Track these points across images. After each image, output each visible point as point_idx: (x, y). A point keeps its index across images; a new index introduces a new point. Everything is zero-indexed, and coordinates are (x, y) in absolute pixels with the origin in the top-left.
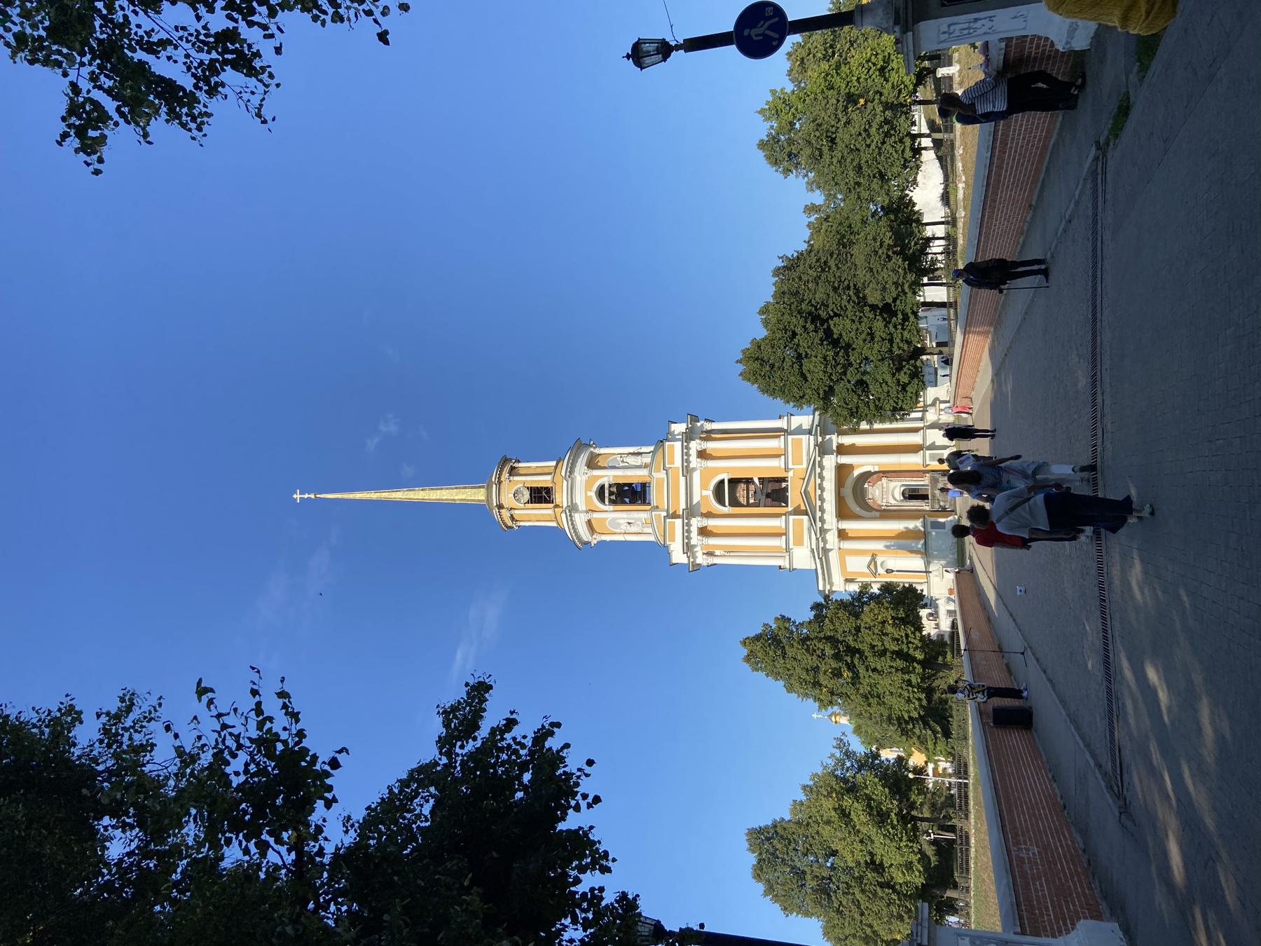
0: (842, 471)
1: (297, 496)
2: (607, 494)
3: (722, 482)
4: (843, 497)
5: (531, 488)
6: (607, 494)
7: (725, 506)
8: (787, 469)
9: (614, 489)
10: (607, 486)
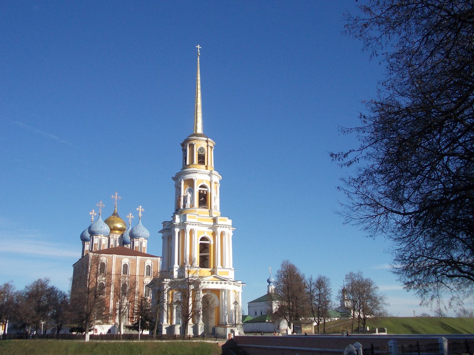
0: (217, 292)
1: (199, 47)
3: (210, 242)
5: (205, 155)
7: (201, 240)
10: (206, 189)
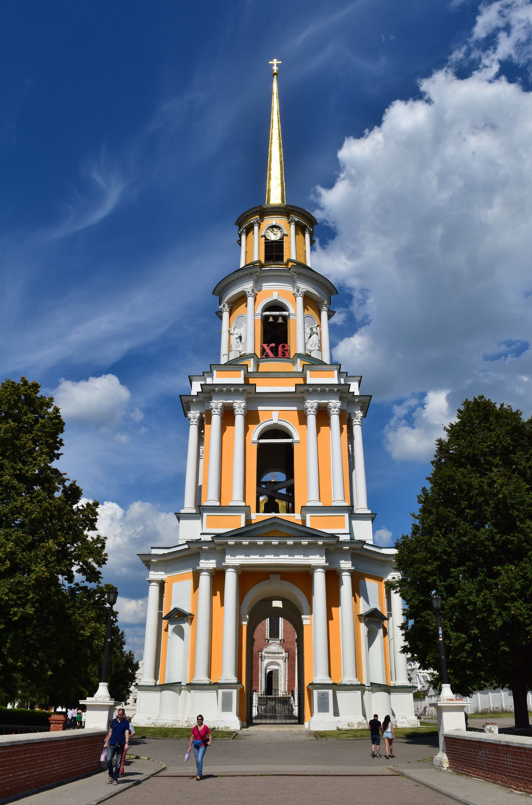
2: (274, 313)
3: (288, 435)
4: (269, 579)
6: (274, 313)
7: (261, 437)
8: (305, 509)
9: (280, 320)
